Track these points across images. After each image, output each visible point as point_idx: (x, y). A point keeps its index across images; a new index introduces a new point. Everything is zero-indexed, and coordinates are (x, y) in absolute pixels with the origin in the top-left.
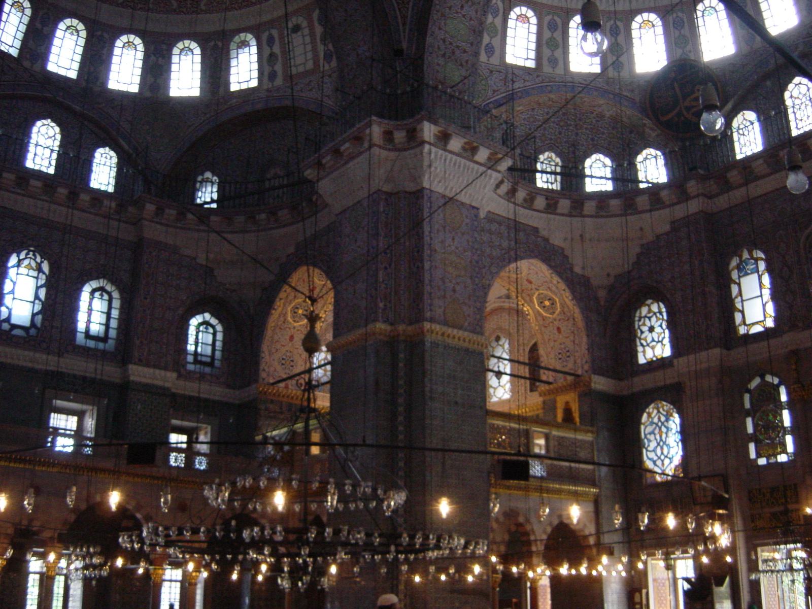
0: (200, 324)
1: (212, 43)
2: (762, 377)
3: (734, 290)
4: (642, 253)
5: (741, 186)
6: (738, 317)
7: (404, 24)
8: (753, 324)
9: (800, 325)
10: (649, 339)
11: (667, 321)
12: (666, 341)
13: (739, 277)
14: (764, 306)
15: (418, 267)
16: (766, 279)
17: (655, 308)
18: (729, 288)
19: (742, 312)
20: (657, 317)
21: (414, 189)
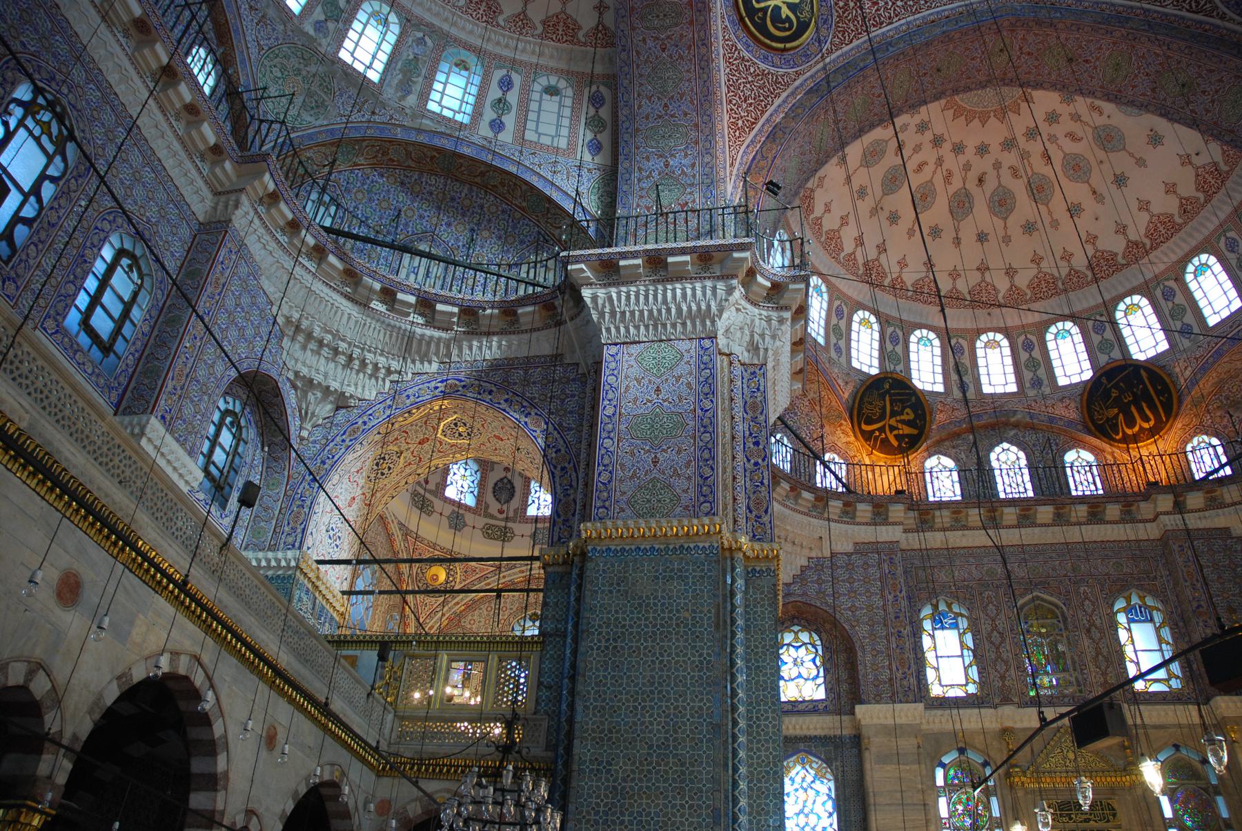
0: (227, 413)
1: (420, 35)
2: (962, 751)
3: (926, 642)
4: (808, 567)
5: (944, 530)
6: (931, 675)
7: (732, 165)
8: (952, 686)
9: (1016, 700)
10: (794, 673)
11: (823, 657)
12: (820, 680)
13: (934, 629)
14: (966, 669)
15: (756, 464)
16: (969, 639)
17: (804, 637)
18: (921, 638)
19: (937, 669)
20: (807, 649)
21: (747, 361)
